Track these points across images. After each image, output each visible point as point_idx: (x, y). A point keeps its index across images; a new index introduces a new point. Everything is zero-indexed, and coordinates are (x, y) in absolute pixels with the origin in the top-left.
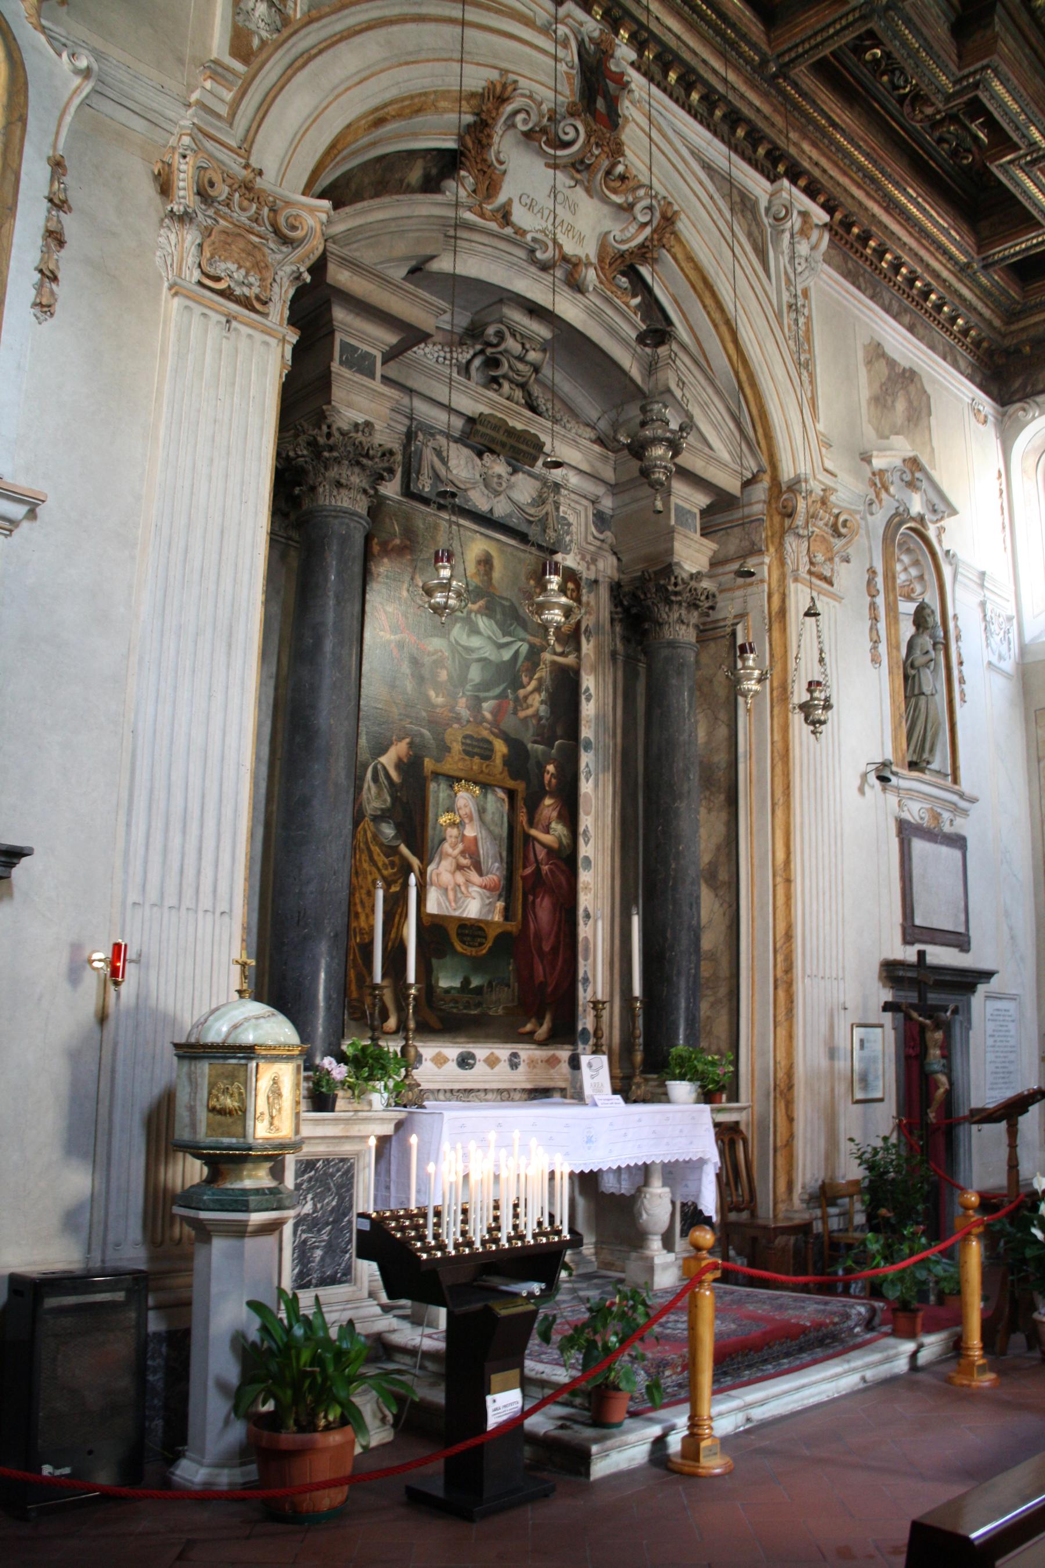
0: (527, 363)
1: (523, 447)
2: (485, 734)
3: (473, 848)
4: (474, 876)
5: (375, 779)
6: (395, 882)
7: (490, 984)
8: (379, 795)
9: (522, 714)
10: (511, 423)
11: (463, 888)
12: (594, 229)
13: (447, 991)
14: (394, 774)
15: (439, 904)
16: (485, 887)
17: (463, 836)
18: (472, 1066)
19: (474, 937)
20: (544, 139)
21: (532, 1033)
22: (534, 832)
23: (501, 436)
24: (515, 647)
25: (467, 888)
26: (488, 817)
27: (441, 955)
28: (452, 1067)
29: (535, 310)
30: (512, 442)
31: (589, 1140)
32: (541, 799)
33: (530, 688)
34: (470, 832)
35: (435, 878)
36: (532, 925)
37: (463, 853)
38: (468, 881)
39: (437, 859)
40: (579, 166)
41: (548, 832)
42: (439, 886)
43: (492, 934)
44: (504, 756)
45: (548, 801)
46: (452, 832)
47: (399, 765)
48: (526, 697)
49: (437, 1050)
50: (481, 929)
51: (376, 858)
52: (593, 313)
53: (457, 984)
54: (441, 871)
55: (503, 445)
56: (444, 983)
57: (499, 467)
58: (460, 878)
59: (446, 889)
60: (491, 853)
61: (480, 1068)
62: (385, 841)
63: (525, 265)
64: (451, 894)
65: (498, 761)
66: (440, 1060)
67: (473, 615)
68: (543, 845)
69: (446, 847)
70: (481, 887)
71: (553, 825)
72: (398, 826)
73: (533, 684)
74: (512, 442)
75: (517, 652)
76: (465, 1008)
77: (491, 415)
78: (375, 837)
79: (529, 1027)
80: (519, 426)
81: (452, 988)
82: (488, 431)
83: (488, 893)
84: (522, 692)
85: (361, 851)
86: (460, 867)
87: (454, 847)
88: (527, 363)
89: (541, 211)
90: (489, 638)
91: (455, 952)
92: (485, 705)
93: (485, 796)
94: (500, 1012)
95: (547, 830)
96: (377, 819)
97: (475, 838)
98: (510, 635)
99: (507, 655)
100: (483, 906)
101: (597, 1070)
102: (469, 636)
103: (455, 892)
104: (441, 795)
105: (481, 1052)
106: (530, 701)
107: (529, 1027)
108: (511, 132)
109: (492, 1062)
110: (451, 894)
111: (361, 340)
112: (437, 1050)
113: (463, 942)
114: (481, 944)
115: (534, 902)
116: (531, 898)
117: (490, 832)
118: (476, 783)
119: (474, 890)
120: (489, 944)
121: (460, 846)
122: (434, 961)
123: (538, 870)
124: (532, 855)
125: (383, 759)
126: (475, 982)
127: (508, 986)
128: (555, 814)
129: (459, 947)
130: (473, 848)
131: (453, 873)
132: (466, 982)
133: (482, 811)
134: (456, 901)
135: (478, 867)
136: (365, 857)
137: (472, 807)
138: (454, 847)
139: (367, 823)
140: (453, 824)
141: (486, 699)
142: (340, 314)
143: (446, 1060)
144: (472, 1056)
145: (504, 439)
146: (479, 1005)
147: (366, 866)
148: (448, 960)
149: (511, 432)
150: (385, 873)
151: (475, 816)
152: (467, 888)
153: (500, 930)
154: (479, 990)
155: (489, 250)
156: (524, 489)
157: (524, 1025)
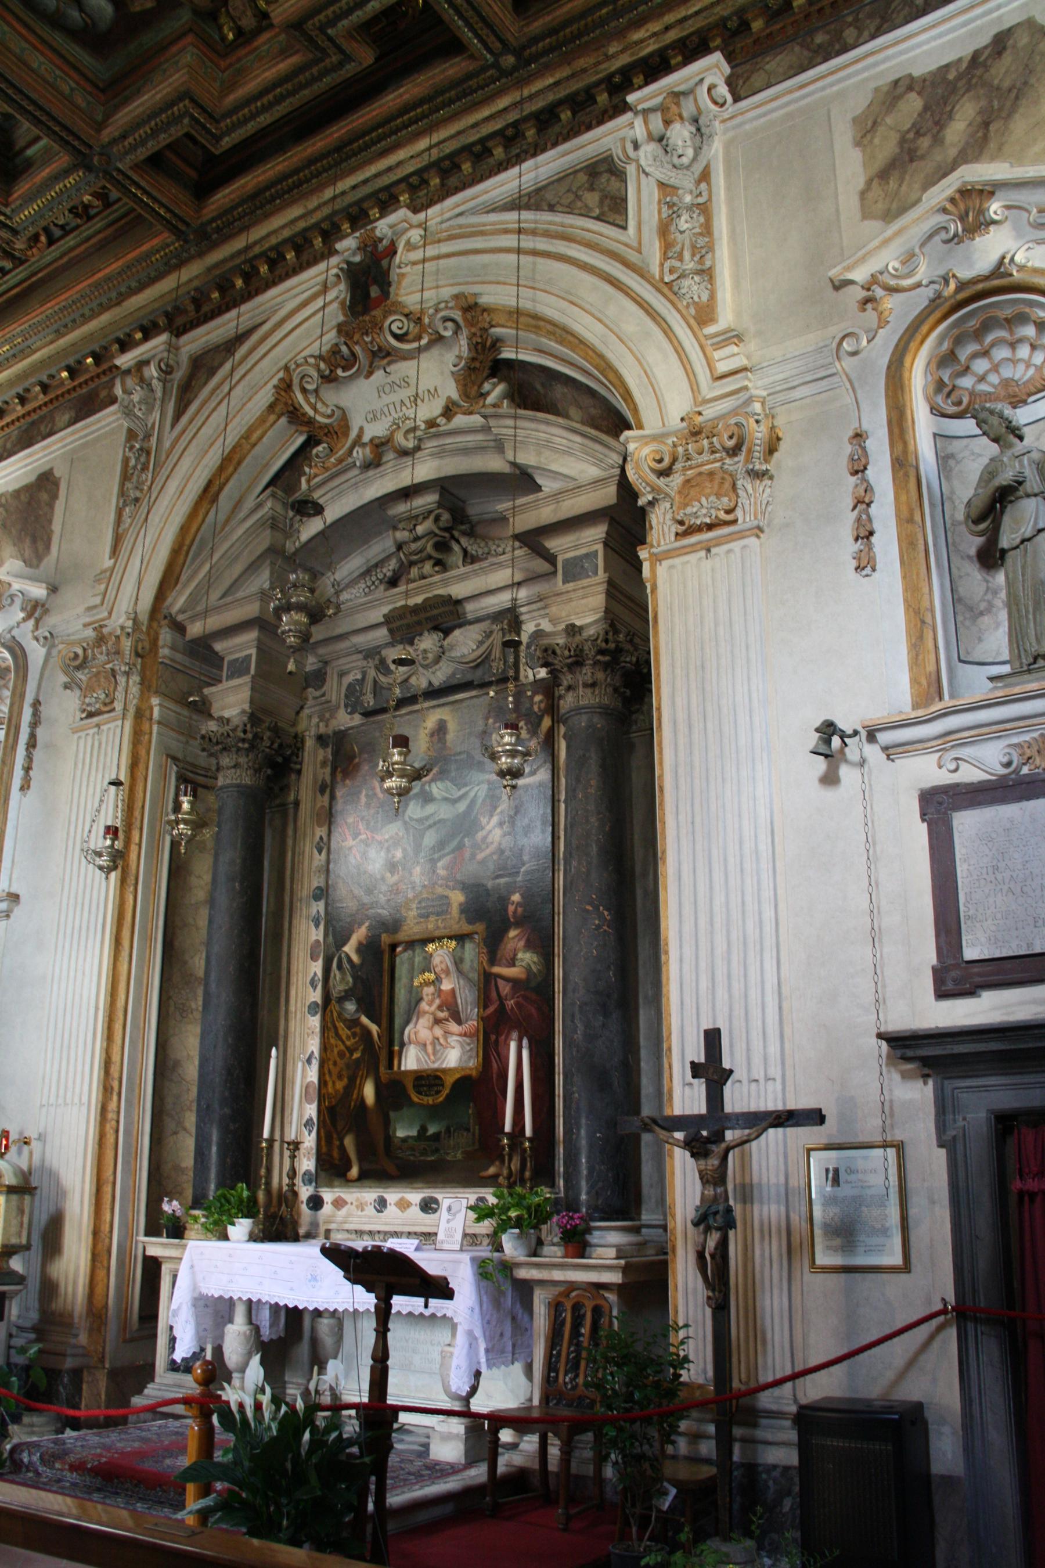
0: (423, 537)
1: (436, 612)
2: (440, 890)
3: (450, 999)
4: (453, 1027)
5: (340, 967)
6: (356, 1049)
7: (448, 1130)
8: (343, 979)
9: (480, 856)
10: (411, 602)
11: (442, 1041)
12: (442, 373)
13: (404, 1140)
14: (355, 958)
15: (418, 1060)
16: (465, 1035)
17: (440, 990)
18: (435, 1211)
19: (430, 1086)
20: (340, 372)
21: (496, 1176)
22: (496, 970)
23: (411, 619)
24: (472, 794)
25: (446, 1039)
26: (466, 966)
27: (398, 1107)
28: (415, 1211)
29: (406, 493)
30: (423, 615)
31: (314, 1278)
32: (506, 931)
33: (488, 828)
34: (446, 986)
35: (413, 1036)
36: (495, 1065)
37: (440, 1008)
38: (447, 1033)
39: (414, 1019)
40: (382, 356)
41: (514, 965)
42: (417, 1043)
43: (449, 1080)
44: (461, 905)
45: (512, 933)
46: (429, 990)
47: (360, 949)
48: (485, 838)
49: (400, 1195)
50: (439, 1078)
51: (341, 1032)
52: (440, 453)
53: (414, 1133)
54: (420, 1029)
55: (419, 623)
56: (400, 1133)
57: (428, 642)
58: (438, 1031)
59: (425, 1045)
60: (469, 999)
61: (391, 1210)
62: (348, 1017)
63: (362, 477)
64: (430, 1049)
65: (455, 910)
66: (403, 1205)
67: (427, 787)
68: (506, 979)
69: (424, 1006)
70: (460, 1035)
71: (520, 955)
72: (359, 1002)
73: (495, 820)
74: (423, 615)
75: (473, 802)
76: (422, 1155)
77: (426, 600)
78: (340, 1015)
79: (492, 1170)
80: (419, 600)
81: (408, 1137)
82: (398, 623)
83: (468, 1040)
84: (480, 835)
85: (329, 1030)
86: (437, 1021)
87: (430, 1004)
88: (423, 537)
89: (383, 413)
90: (446, 799)
91: (411, 1103)
92: (440, 864)
93: (463, 947)
94: (459, 1156)
95: (512, 963)
96: (341, 1000)
97: (453, 991)
98: (466, 785)
99: (462, 807)
100: (463, 1053)
101: (454, 1215)
102: (423, 807)
103: (433, 1044)
104: (417, 960)
105: (392, 1196)
106: (490, 839)
107: (492, 1170)
108: (322, 393)
109: (403, 1205)
110: (430, 1049)
111: (241, 650)
112: (400, 1195)
113: (420, 1093)
114: (438, 1092)
115: (497, 1041)
116: (493, 1037)
117: (469, 980)
118: (450, 938)
119: (453, 1040)
120: (446, 1091)
121: (437, 1002)
122: (392, 1114)
123: (502, 1005)
124: (494, 994)
125: (346, 949)
126: (432, 1130)
127: (468, 1130)
128: (522, 943)
129: (415, 1098)
130: (450, 999)
131: (431, 1029)
132: (423, 1129)
133: (458, 962)
134: (435, 1053)
135: (456, 1017)
136: (332, 1034)
137: (449, 962)
138: (430, 1004)
139: (334, 1006)
140: (427, 983)
141: (439, 859)
142: (219, 647)
143: (409, 1205)
144: (436, 1201)
145: (415, 618)
146: (437, 1150)
147: (332, 1041)
148: (406, 1111)
149: (416, 610)
150: (348, 1043)
151: (452, 968)
152: (446, 1039)
153: (457, 1076)
154: (436, 1137)
155: (329, 495)
156: (466, 642)
157: (487, 1169)
